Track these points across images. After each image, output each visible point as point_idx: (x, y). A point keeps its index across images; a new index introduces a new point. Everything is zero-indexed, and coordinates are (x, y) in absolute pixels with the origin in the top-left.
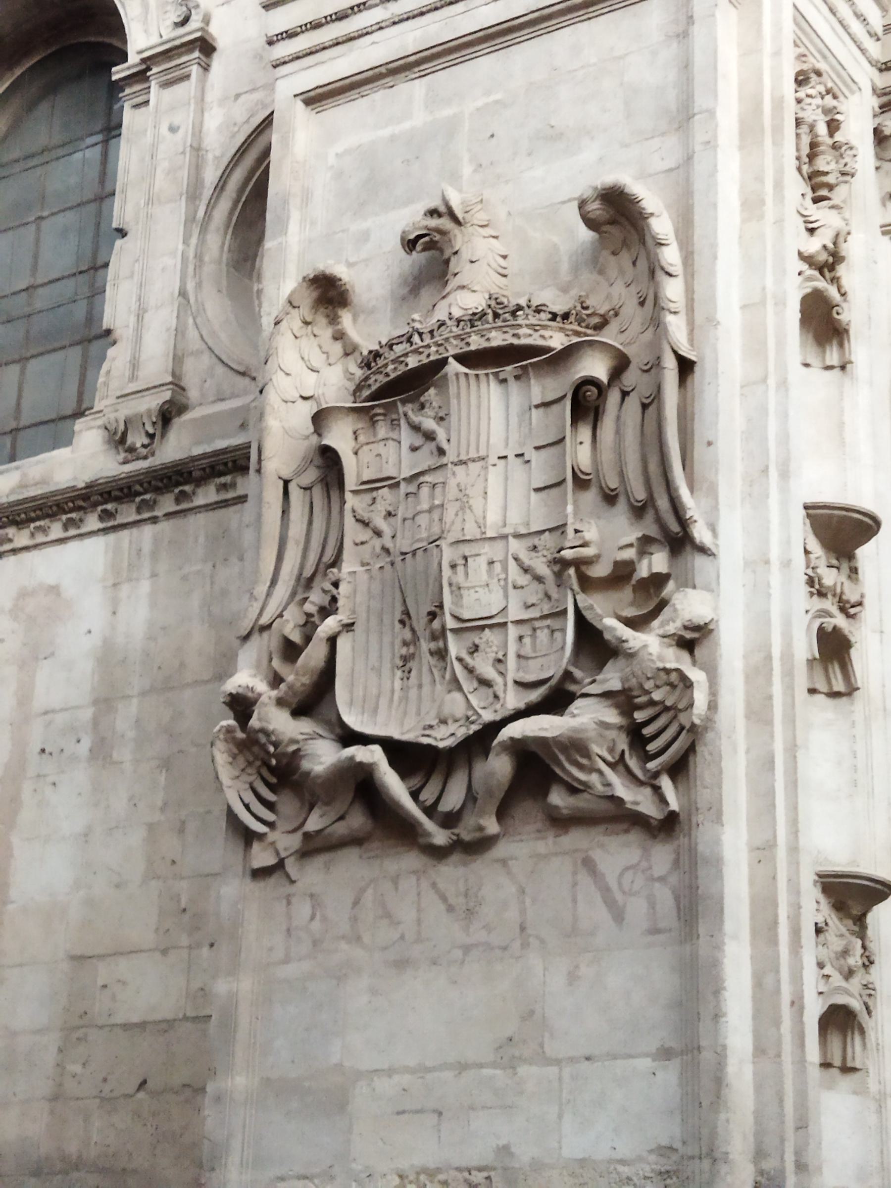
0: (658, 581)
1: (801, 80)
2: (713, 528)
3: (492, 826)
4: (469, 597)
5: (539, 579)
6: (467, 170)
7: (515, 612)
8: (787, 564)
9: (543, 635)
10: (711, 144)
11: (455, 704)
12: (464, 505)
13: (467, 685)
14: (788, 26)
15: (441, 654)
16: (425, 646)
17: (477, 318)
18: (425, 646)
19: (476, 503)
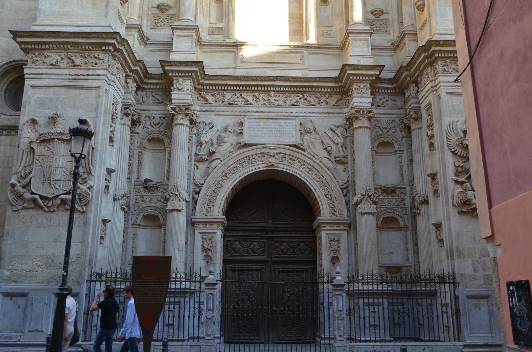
0: (86, 178)
1: (113, 104)
2: (95, 172)
3: (56, 209)
4: (56, 176)
5: (67, 175)
6: (60, 107)
7: (63, 179)
8: (103, 177)
9: (67, 183)
10: (100, 116)
11: (52, 191)
12: (56, 162)
13: (54, 188)
14: (112, 97)
15: (50, 183)
16: (47, 182)
17: (60, 134)
18: (47, 182)
19: (58, 162)
